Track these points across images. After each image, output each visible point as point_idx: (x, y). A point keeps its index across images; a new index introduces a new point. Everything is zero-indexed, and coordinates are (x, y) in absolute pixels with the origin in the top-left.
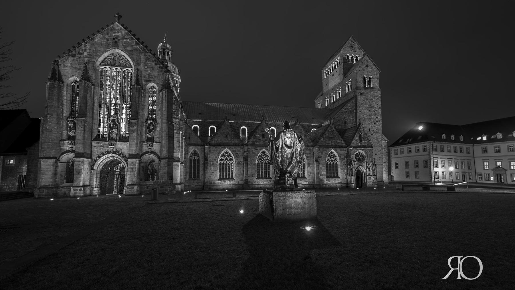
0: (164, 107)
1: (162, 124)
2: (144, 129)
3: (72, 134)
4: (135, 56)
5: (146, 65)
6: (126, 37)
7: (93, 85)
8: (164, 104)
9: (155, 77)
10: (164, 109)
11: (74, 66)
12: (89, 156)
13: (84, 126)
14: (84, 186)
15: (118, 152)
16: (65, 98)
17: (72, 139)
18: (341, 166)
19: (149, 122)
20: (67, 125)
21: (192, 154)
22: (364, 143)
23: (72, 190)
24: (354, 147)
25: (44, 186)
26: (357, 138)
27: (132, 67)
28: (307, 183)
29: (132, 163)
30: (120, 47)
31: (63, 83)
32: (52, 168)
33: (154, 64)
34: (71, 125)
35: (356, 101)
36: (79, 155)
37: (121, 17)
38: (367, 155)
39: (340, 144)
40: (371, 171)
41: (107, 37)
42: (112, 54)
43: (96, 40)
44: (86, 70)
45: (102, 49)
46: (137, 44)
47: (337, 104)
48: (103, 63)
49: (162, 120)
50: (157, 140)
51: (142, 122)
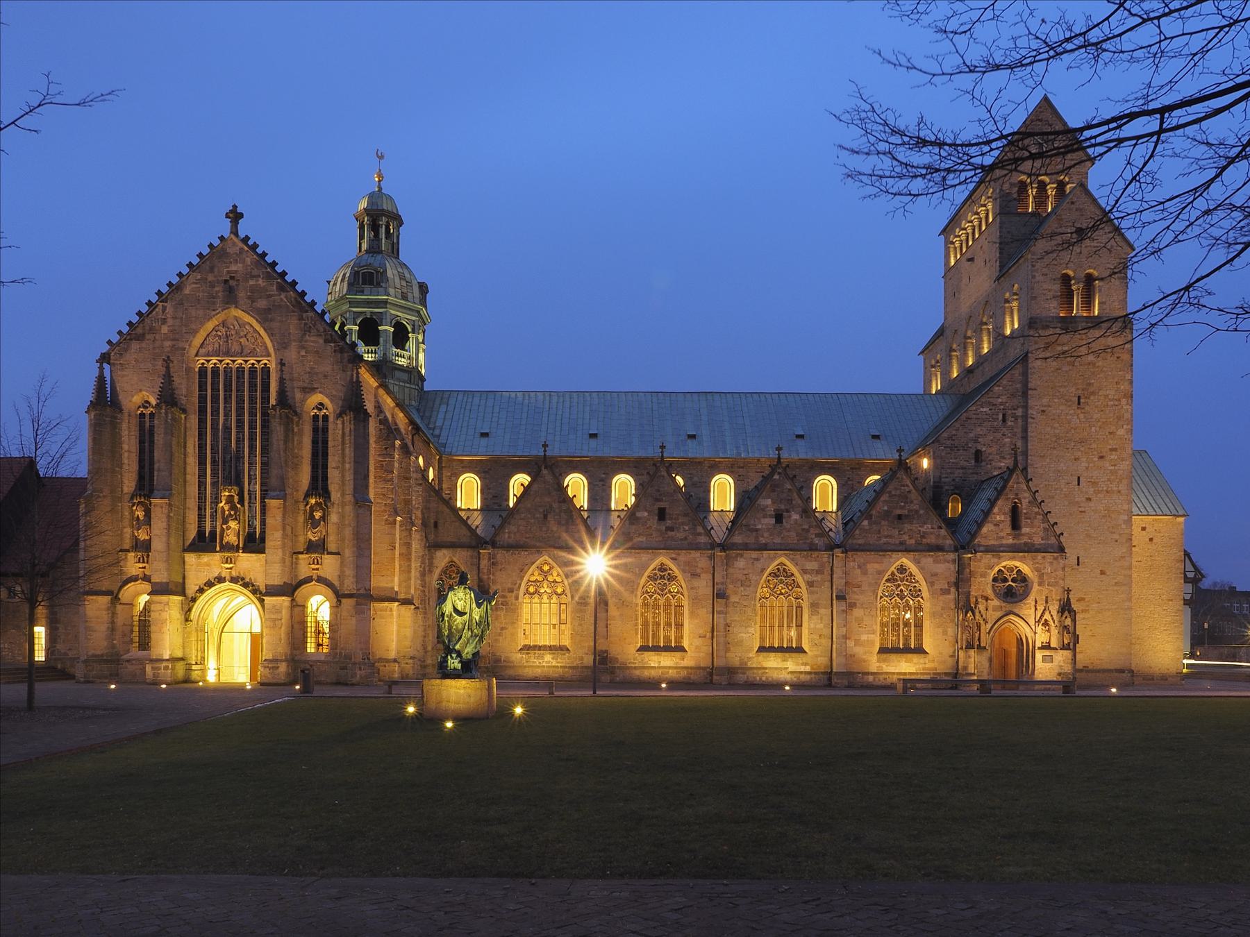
0: (347, 459)
1: (343, 504)
2: (301, 519)
3: (142, 536)
4: (275, 325)
5: (303, 347)
6: (255, 272)
7: (184, 411)
8: (347, 451)
9: (326, 376)
10: (347, 466)
11: (142, 366)
12: (180, 589)
13: (169, 517)
14: (173, 660)
15: (243, 579)
16: (125, 447)
17: (144, 548)
18: (934, 615)
19: (313, 501)
20: (132, 513)
21: (444, 572)
22: (1030, 536)
23: (148, 668)
24: (988, 550)
25: (94, 655)
26: (1000, 514)
27: (269, 355)
28: (808, 669)
29: (274, 606)
30: (241, 302)
31: (121, 410)
32: (105, 616)
33: (321, 341)
34: (140, 514)
35: (1025, 374)
36: (159, 590)
37: (241, 215)
38: (1041, 576)
39: (932, 540)
40: (1054, 631)
41: (211, 277)
42: (224, 324)
43: (187, 291)
44: (168, 377)
45: (201, 313)
46: (281, 289)
47: (978, 380)
48: (202, 351)
49: (343, 495)
50: (332, 547)
51: (297, 502)
